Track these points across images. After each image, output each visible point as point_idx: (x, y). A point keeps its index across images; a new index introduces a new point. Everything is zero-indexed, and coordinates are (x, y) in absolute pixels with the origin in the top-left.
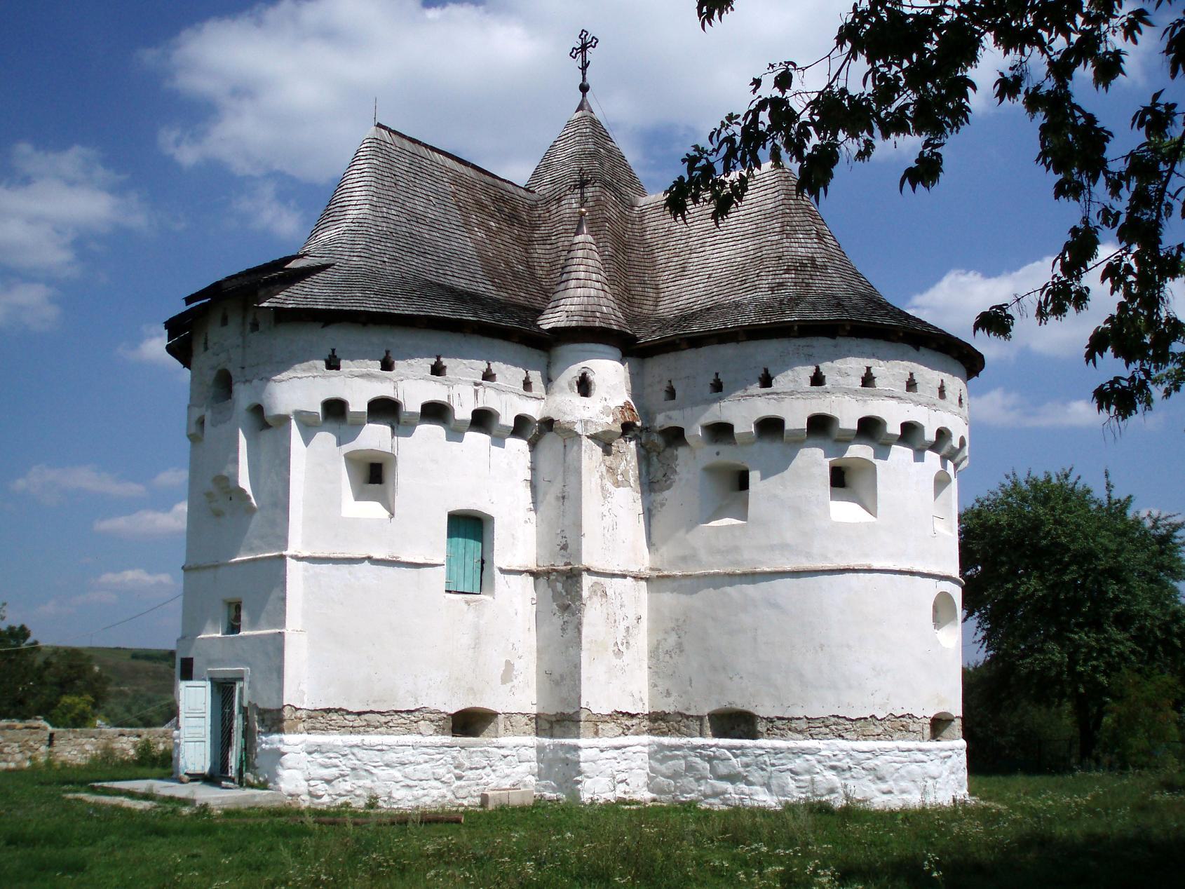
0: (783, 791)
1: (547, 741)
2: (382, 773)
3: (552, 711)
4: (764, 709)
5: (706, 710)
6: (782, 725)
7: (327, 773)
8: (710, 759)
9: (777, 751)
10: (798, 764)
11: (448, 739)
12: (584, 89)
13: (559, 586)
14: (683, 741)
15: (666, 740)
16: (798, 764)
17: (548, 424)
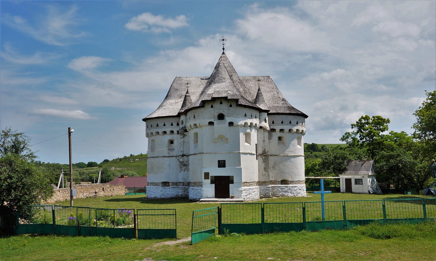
0: (293, 194)
1: (261, 187)
2: (253, 193)
3: (262, 181)
4: (290, 180)
5: (280, 180)
6: (292, 182)
7: (247, 194)
8: (281, 189)
9: (292, 187)
10: (295, 189)
11: (257, 187)
12: (223, 49)
13: (264, 158)
14: (276, 185)
15: (273, 185)
16: (295, 189)
17: (261, 127)
